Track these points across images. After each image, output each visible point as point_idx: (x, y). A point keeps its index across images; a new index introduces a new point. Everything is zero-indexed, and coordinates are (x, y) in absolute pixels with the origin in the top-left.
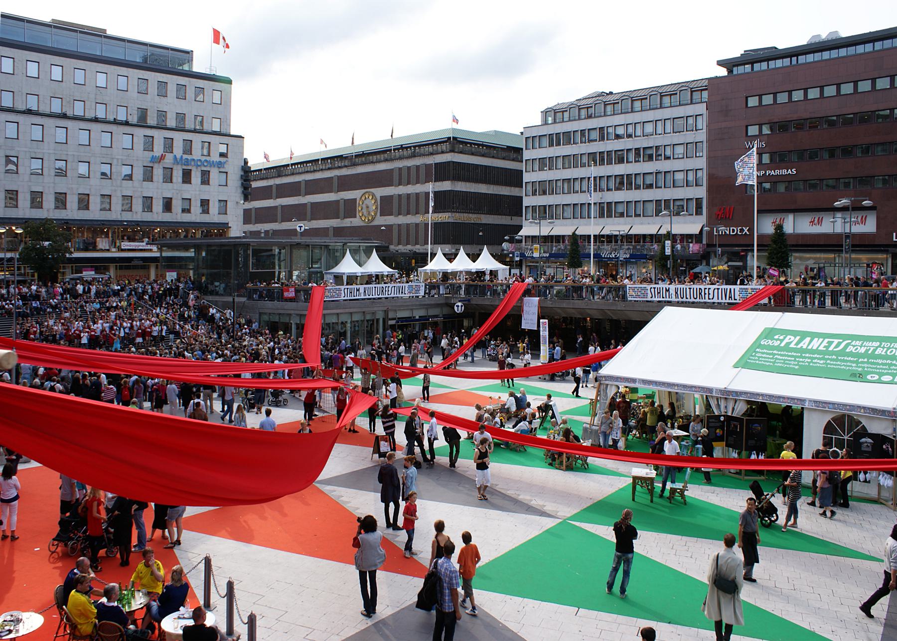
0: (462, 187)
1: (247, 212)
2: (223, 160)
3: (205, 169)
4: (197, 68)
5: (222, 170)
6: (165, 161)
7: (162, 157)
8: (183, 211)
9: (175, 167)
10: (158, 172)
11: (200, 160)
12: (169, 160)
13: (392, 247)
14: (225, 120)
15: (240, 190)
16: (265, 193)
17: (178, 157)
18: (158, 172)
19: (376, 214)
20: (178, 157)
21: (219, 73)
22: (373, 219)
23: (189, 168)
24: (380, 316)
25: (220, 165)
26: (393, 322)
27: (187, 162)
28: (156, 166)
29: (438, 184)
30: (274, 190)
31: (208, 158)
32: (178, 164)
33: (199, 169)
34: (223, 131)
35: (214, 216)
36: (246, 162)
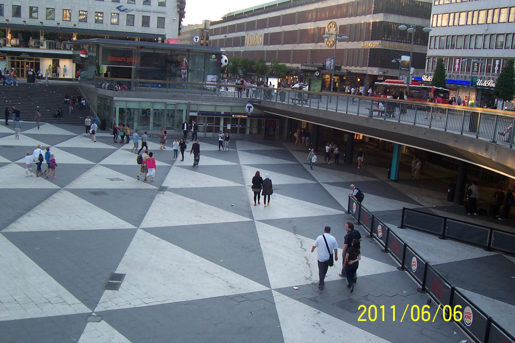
8: (97, 21)
13: (343, 67)
15: (176, 10)
24: (184, 108)
26: (195, 114)
35: (153, 29)
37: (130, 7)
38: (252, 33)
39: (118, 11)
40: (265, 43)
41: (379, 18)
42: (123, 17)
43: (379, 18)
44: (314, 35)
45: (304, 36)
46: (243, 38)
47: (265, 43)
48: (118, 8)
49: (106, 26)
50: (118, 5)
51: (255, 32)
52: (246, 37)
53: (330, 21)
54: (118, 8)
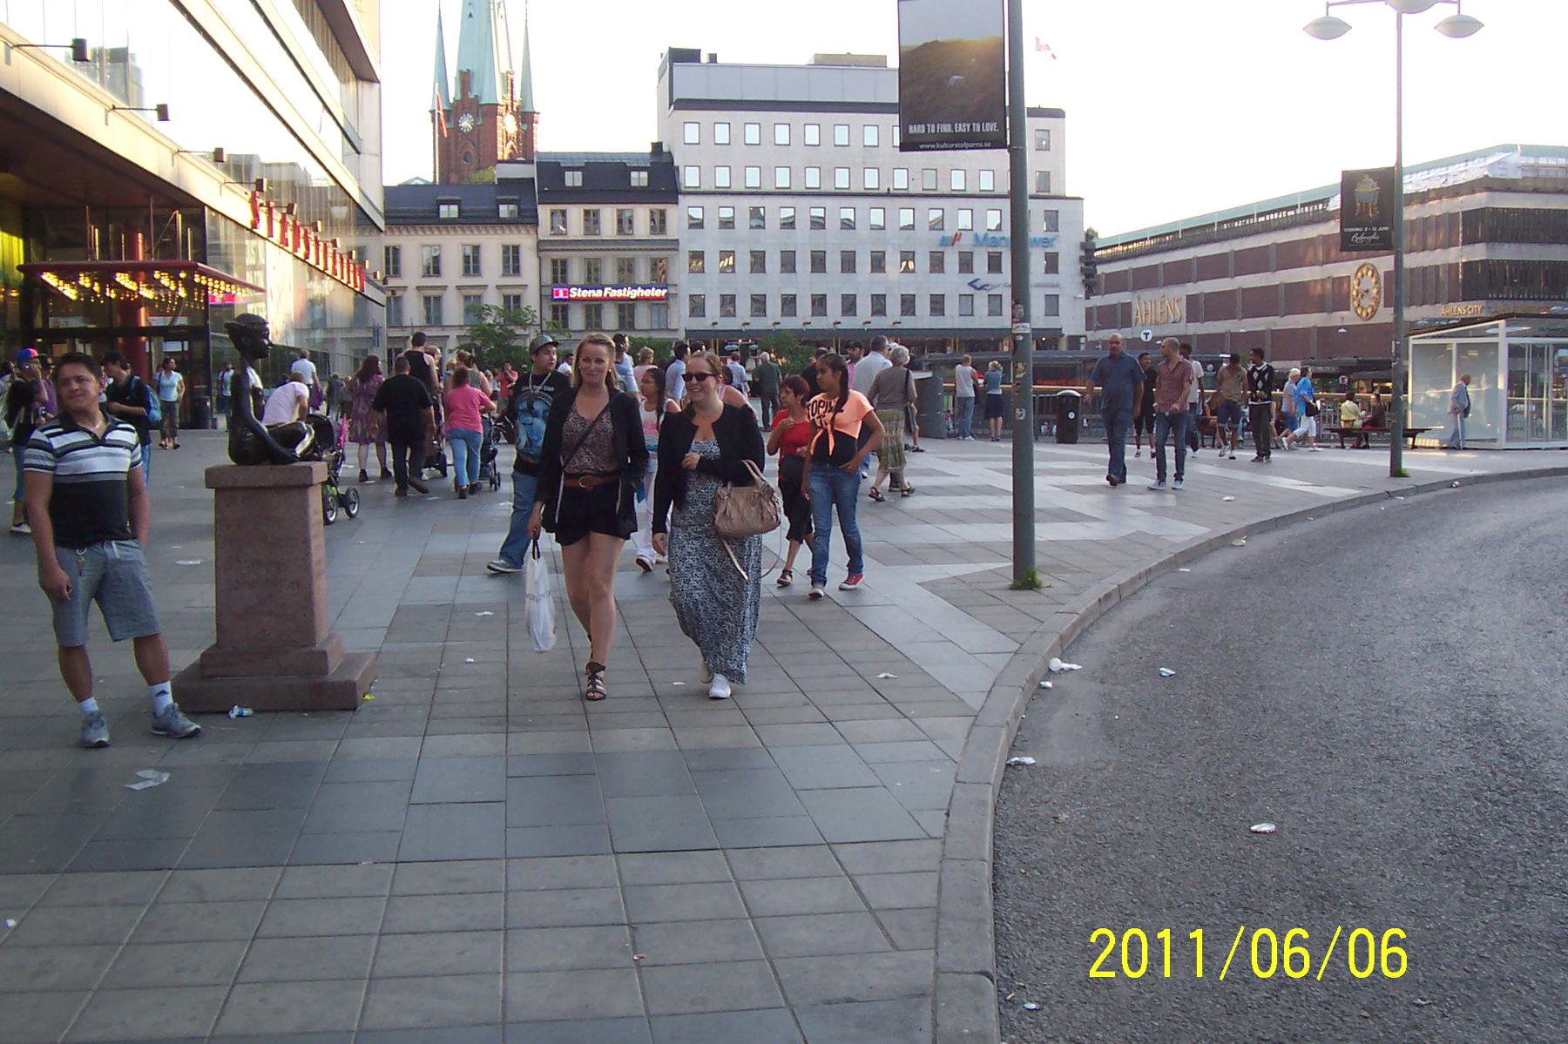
0: (1508, 252)
1: (1089, 311)
2: (1050, 235)
10: (952, 260)
12: (966, 243)
15: (1081, 278)
16: (1117, 283)
17: (981, 234)
18: (952, 260)
19: (1377, 303)
20: (981, 234)
21: (1045, 105)
22: (1374, 311)
25: (1046, 242)
29: (1468, 248)
30: (1161, 274)
37: (994, 278)
38: (1148, 295)
39: (970, 291)
40: (1192, 317)
41: (1479, 252)
42: (981, 301)
43: (1479, 252)
44: (1322, 296)
45: (1298, 298)
46: (1127, 307)
47: (1192, 317)
48: (970, 284)
49: (952, 320)
50: (970, 278)
51: (1162, 291)
52: (1135, 306)
53: (1362, 262)
54: (970, 284)
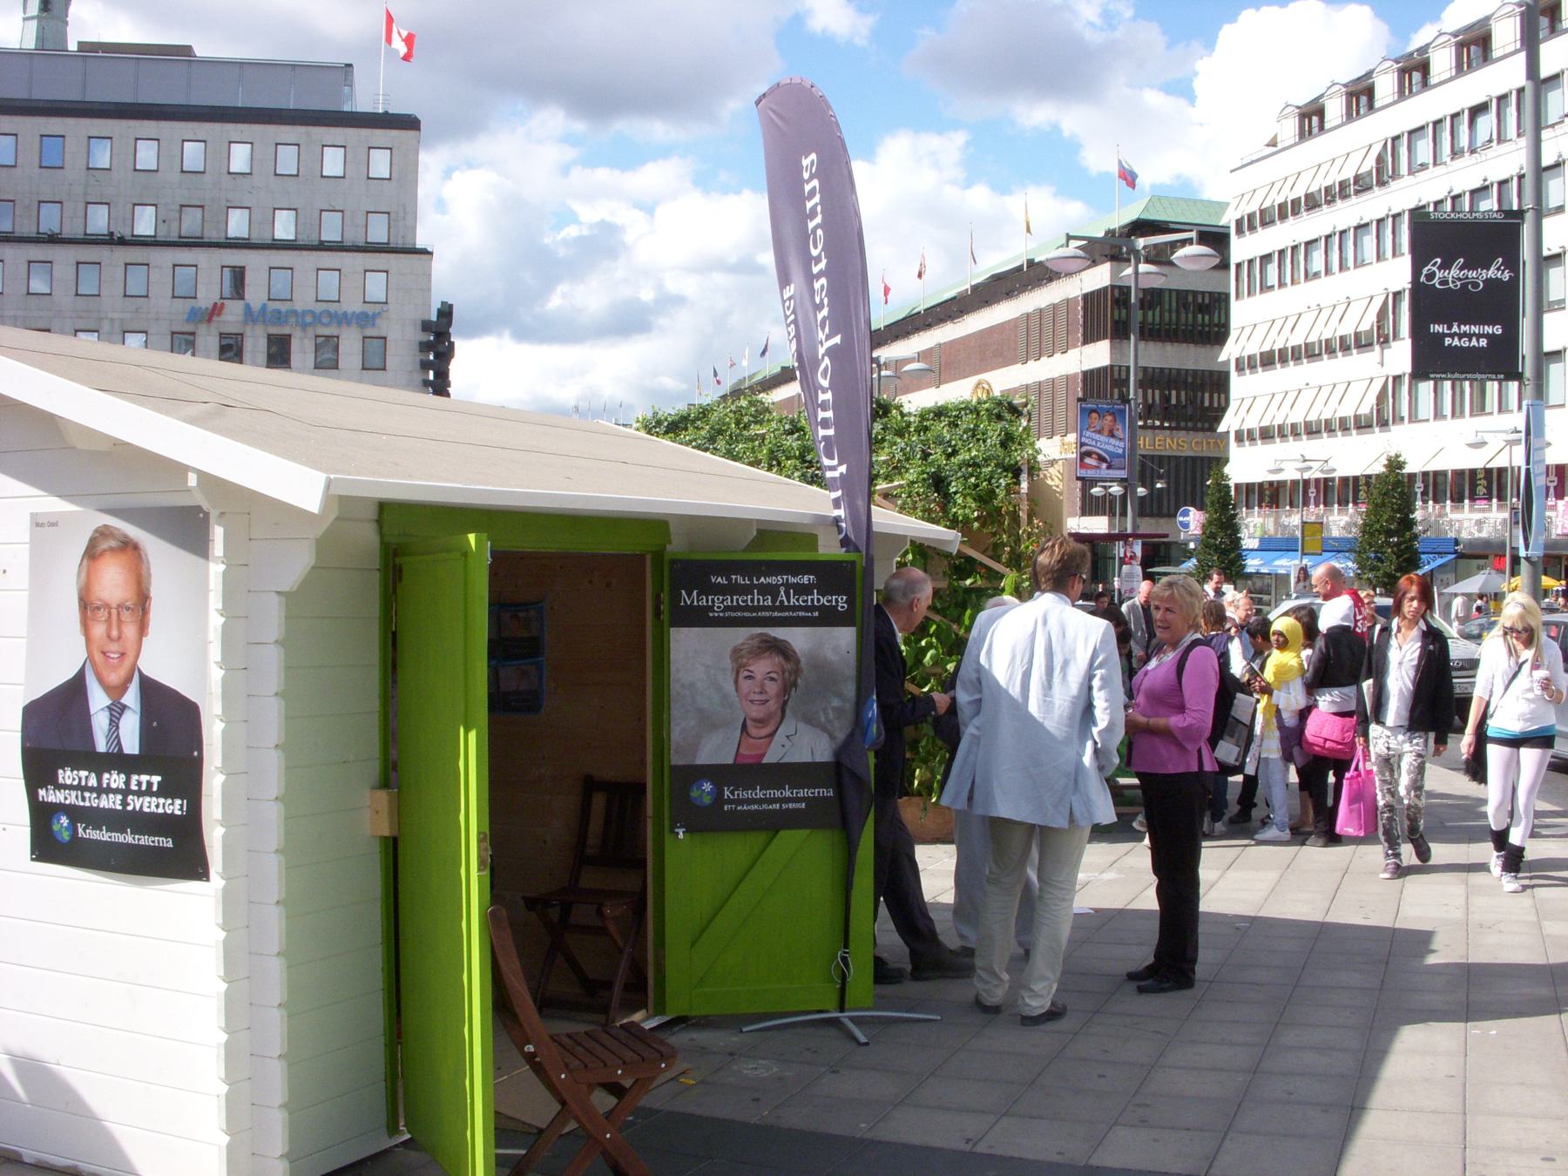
3: (327, 331)
4: (364, 100)
5: (370, 332)
6: (224, 317)
7: (216, 310)
9: (248, 331)
11: (312, 313)
14: (403, 211)
21: (396, 109)
23: (286, 331)
27: (279, 318)
28: (202, 330)
31: (333, 308)
32: (254, 321)
33: (311, 332)
34: (397, 242)
36: (446, 313)
